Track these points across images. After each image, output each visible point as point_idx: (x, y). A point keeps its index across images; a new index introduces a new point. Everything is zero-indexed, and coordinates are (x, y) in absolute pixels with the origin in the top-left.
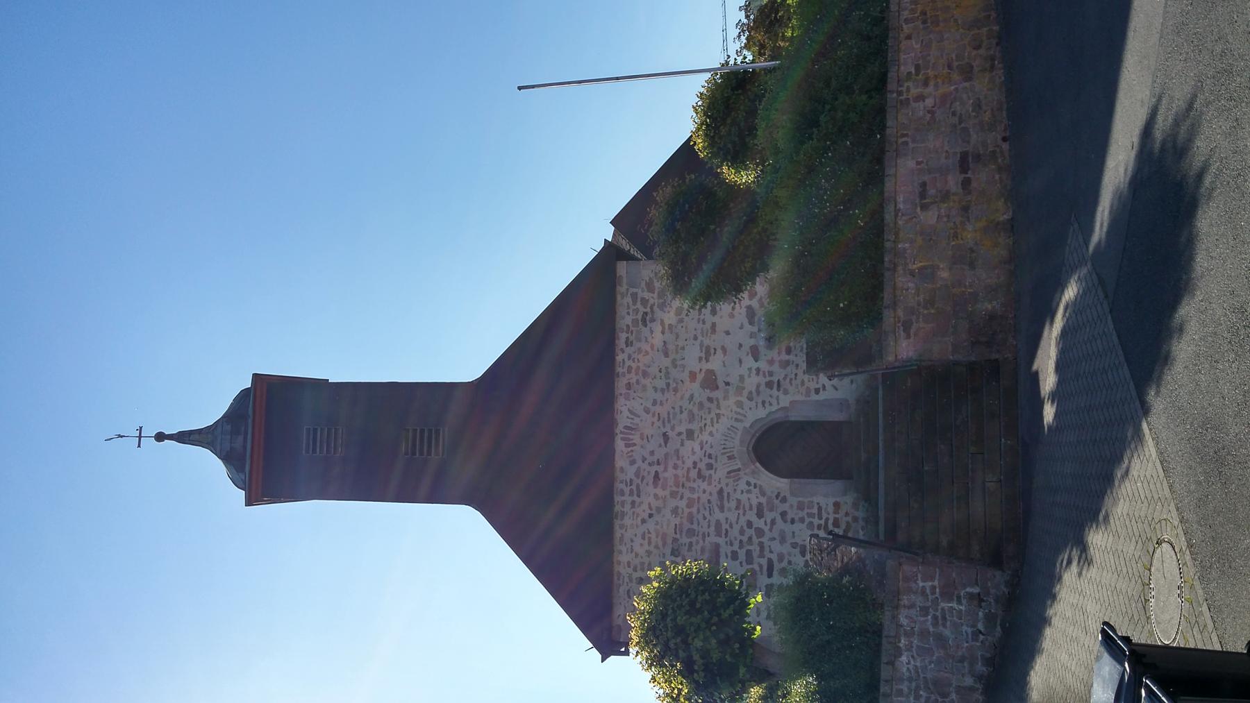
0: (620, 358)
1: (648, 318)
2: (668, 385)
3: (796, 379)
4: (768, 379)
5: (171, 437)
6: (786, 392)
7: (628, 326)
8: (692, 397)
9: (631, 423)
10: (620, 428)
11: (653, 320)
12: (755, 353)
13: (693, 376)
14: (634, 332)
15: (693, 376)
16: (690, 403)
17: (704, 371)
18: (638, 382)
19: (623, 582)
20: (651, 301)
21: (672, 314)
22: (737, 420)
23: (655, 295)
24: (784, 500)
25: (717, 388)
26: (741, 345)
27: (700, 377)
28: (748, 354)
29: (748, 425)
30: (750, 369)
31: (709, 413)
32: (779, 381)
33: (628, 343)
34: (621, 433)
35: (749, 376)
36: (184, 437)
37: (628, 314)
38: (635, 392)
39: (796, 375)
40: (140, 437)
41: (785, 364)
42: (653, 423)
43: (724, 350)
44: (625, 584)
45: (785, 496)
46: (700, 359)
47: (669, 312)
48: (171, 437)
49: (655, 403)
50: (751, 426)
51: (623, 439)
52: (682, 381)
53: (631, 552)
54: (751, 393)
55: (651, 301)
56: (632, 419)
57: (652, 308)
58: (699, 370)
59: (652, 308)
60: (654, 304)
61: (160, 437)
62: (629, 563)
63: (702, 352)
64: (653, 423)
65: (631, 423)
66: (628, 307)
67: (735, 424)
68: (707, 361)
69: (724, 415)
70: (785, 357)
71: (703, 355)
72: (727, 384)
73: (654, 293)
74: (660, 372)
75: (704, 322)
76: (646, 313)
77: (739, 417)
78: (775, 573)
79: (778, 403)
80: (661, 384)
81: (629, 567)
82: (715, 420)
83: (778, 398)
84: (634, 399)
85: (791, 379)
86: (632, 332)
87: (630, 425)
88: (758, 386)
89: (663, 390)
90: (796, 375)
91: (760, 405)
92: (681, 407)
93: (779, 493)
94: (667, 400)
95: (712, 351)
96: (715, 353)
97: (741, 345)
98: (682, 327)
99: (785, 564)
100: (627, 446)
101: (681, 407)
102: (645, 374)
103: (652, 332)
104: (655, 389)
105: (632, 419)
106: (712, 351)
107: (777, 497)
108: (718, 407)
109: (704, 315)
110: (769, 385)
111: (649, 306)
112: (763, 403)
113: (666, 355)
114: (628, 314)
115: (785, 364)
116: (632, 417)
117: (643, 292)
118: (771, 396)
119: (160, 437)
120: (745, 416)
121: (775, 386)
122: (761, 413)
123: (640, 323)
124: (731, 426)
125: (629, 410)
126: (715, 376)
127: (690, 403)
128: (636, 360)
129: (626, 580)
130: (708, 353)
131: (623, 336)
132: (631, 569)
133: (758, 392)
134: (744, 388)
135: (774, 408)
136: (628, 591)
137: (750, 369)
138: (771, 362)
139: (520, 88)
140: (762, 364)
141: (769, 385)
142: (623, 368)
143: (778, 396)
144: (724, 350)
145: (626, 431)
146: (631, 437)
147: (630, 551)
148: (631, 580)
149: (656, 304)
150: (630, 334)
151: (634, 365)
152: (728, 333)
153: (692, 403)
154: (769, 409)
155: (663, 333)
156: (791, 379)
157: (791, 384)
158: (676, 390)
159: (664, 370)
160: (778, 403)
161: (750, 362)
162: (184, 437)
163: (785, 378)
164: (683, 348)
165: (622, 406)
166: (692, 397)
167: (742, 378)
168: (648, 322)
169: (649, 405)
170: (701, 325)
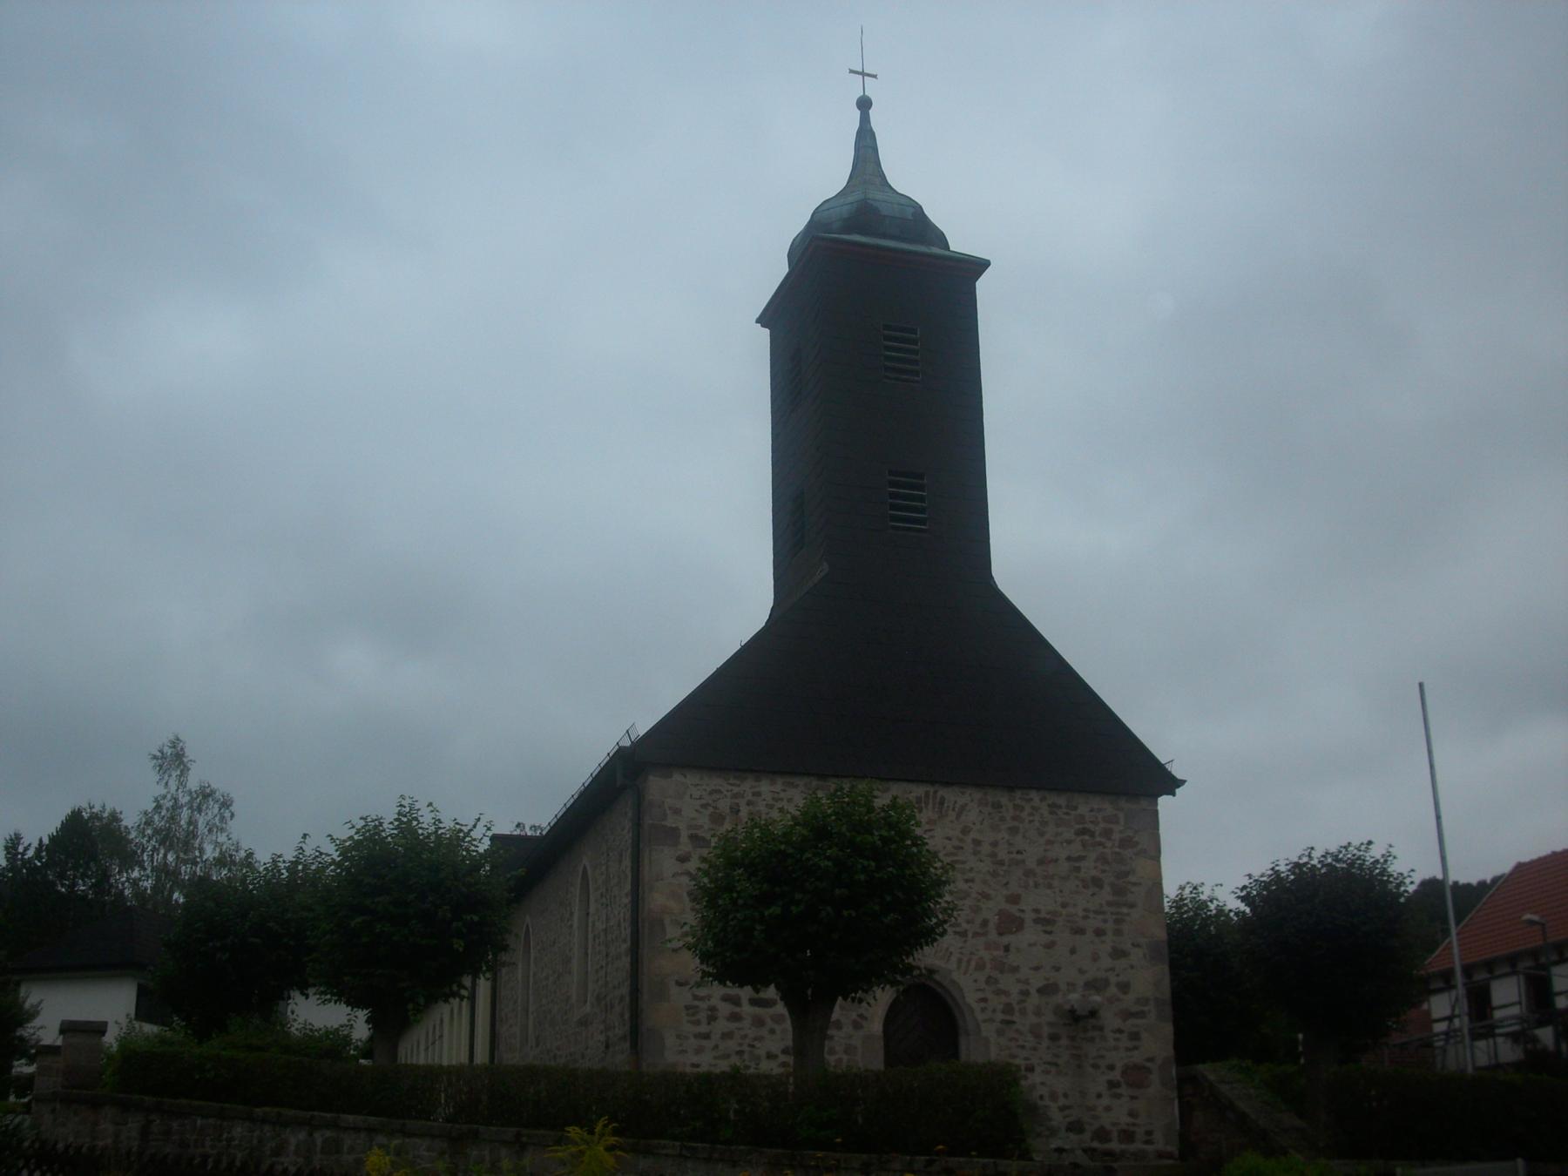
0: (1034, 794)
1: (1087, 837)
2: (1001, 863)
3: (1018, 1046)
4: (1017, 1008)
6: (1000, 1033)
7: (1076, 808)
8: (986, 896)
9: (948, 807)
10: (943, 792)
11: (1084, 845)
12: (1048, 990)
13: (1014, 899)
15: (1014, 899)
16: (980, 894)
17: (1022, 915)
18: (1002, 819)
19: (731, 785)
20: (1109, 844)
21: (1094, 873)
22: (960, 961)
23: (1117, 850)
24: (857, 1026)
25: (1001, 934)
27: (1013, 909)
28: (1047, 979)
29: (955, 976)
30: (1027, 982)
31: (968, 922)
32: (1014, 1022)
33: (1053, 807)
34: (935, 792)
35: (1019, 981)
36: (866, 141)
37: (1092, 811)
38: (990, 814)
39: (1023, 1047)
40: (863, 74)
41: (1035, 1032)
42: (949, 839)
43: (1050, 946)
44: (730, 788)
45: (862, 1027)
46: (1037, 911)
47: (1095, 868)
49: (977, 843)
50: (953, 982)
52: (1007, 883)
53: (773, 799)
55: (1109, 844)
56: (953, 810)
57: (1100, 844)
58: (1024, 908)
59: (1100, 844)
60: (1105, 847)
61: (864, 104)
62: (758, 794)
63: (1048, 913)
64: (949, 839)
65: (948, 807)
66: (1100, 810)
67: (954, 959)
68: (1036, 921)
69: (965, 941)
70: (1046, 1031)
71: (1043, 915)
72: (1007, 949)
73: (1119, 847)
74: (1018, 852)
75: (1085, 918)
76: (1092, 834)
77: (964, 964)
79: (985, 1021)
80: (1002, 854)
81: (754, 794)
82: (958, 929)
83: (991, 1020)
84: (980, 811)
85: (1016, 1040)
86: (1067, 814)
87: (946, 805)
88: (1006, 993)
89: (993, 855)
90: (1023, 1047)
91: (980, 995)
92: (972, 881)
93: (866, 1019)
94: (981, 861)
95: (1049, 928)
96: (1046, 932)
97: (1057, 969)
98: (1077, 886)
99: (770, 1024)
100: (919, 800)
101: (972, 881)
102: (1013, 831)
103: (1069, 842)
104: (995, 844)
105: (953, 810)
106: (1049, 928)
107: (861, 1016)
108: (976, 934)
109: (1094, 918)
110: (1008, 1009)
111: (1103, 840)
112: (984, 1000)
113: (1041, 862)
114: (1092, 811)
115: (1035, 1032)
116: (957, 809)
117: (1121, 832)
118: (994, 1011)
119: (864, 104)
120: (965, 973)
121: (1008, 1018)
122: (971, 998)
123: (1081, 826)
124: (951, 953)
125: (966, 805)
126: (1015, 932)
127: (980, 894)
128: (1031, 818)
129: (736, 790)
130: (1045, 922)
131: (1061, 800)
132: (750, 797)
133: (999, 992)
134: (1002, 972)
135: (980, 1017)
136: (719, 792)
137: (1027, 982)
138: (1038, 1012)
139: (1421, 685)
140: (1034, 1000)
142: (1020, 798)
143: (994, 1021)
144: (1050, 946)
146: (930, 806)
147: (776, 795)
148: (735, 796)
150: (1065, 810)
151: (1024, 815)
152: (1073, 951)
153: (980, 897)
154: (977, 1007)
155: (1069, 859)
156: (1016, 1040)
157: (1011, 1040)
158: (994, 874)
159: (1019, 857)
160: (985, 1021)
161: (1037, 982)
162: (866, 141)
163: (1017, 1031)
164: (1050, 886)
165: (970, 795)
166: (986, 896)
167: (1015, 969)
168: (1082, 837)
169: (973, 835)
170: (1081, 913)
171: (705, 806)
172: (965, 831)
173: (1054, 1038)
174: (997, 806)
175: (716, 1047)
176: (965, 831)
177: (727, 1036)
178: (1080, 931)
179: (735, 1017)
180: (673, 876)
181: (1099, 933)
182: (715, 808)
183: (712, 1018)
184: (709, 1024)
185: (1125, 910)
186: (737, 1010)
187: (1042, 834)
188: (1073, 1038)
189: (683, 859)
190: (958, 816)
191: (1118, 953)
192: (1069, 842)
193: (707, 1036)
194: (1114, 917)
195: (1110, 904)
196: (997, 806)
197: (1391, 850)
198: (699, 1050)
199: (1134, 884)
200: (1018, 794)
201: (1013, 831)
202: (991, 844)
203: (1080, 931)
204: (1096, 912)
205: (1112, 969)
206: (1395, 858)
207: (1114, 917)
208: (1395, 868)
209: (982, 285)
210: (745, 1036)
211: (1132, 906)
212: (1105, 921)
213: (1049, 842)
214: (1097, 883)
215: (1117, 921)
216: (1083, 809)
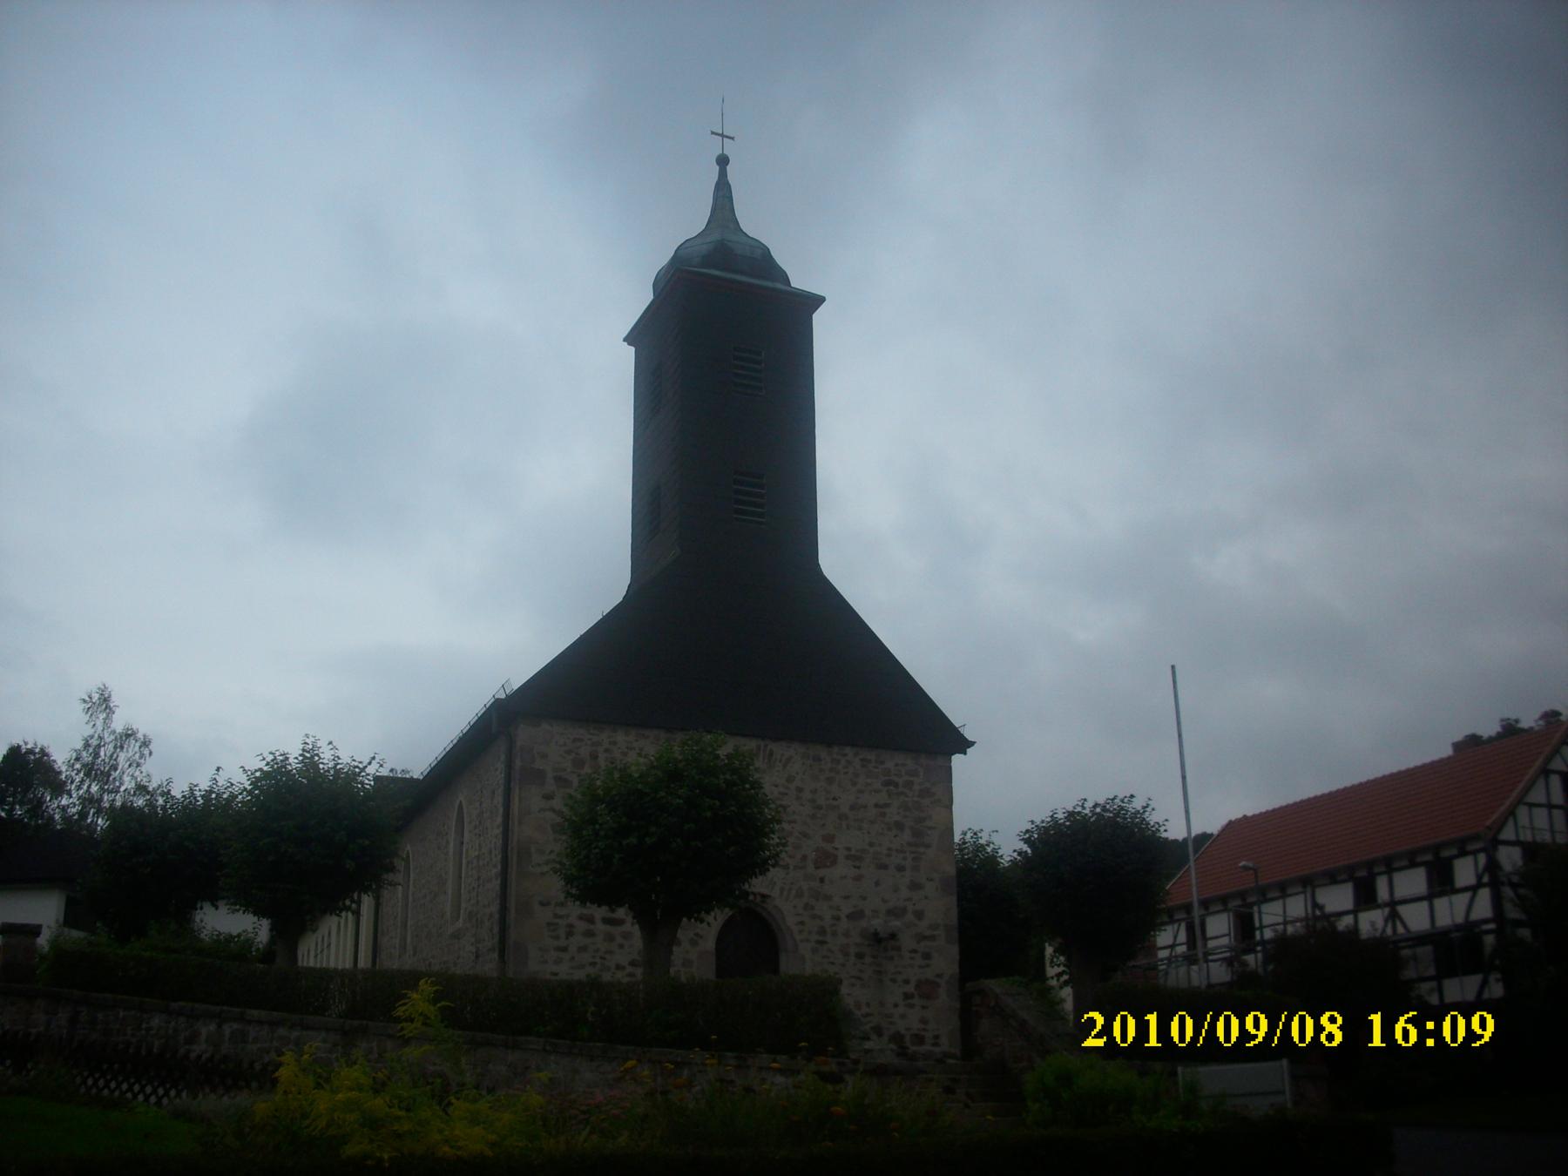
0: (848, 750)
1: (892, 788)
2: (820, 807)
5: (723, 174)
7: (882, 763)
8: (805, 835)
10: (773, 746)
12: (856, 916)
13: (829, 838)
14: (877, 770)
15: (829, 838)
16: (800, 833)
21: (897, 818)
22: (782, 890)
23: (916, 799)
24: (694, 943)
25: (817, 868)
26: (864, 898)
34: (766, 746)
36: (723, 191)
39: (833, 963)
40: (722, 136)
43: (858, 878)
46: (849, 849)
47: (899, 813)
48: (723, 174)
49: (800, 790)
51: (759, 748)
52: (824, 825)
53: (627, 748)
54: (813, 908)
60: (907, 796)
61: (723, 161)
62: (615, 743)
64: (776, 786)
68: (847, 857)
69: (787, 874)
71: (853, 852)
72: (822, 880)
74: (834, 799)
76: (896, 785)
77: (785, 893)
78: (609, 928)
81: (610, 743)
83: (808, 941)
88: (821, 918)
89: (813, 801)
90: (833, 963)
92: (794, 822)
94: (802, 805)
95: (857, 864)
96: (855, 867)
101: (794, 822)
102: (830, 781)
103: (877, 791)
104: (814, 791)
106: (857, 864)
107: (697, 935)
110: (822, 931)
112: (802, 923)
113: (852, 808)
119: (723, 161)
121: (821, 938)
123: (887, 778)
127: (800, 833)
128: (846, 770)
130: (855, 858)
131: (871, 756)
133: (814, 917)
134: (817, 900)
136: (581, 740)
137: (838, 909)
138: (847, 934)
139: (1173, 667)
141: (822, 931)
144: (858, 878)
145: (767, 752)
149: (906, 799)
152: (877, 884)
155: (876, 806)
157: (824, 957)
158: (813, 817)
159: (835, 803)
160: (802, 941)
162: (723, 191)
164: (860, 829)
166: (805, 835)
167: (828, 898)
171: (569, 752)
172: (790, 779)
173: (860, 956)
174: (818, 759)
175: (573, 958)
176: (790, 779)
177: (583, 949)
178: (884, 867)
179: (590, 934)
180: (539, 812)
181: (901, 869)
182: (577, 754)
183: (569, 934)
184: (567, 938)
185: (922, 850)
186: (592, 927)
187: (854, 784)
188: (874, 957)
189: (548, 797)
190: (785, 766)
191: (915, 886)
192: (877, 791)
193: (564, 949)
194: (913, 855)
195: (910, 844)
196: (818, 759)
197: (1150, 802)
198: (558, 962)
199: (930, 828)
200: (836, 749)
201: (830, 781)
202: (811, 791)
203: (884, 867)
204: (897, 850)
205: (910, 899)
206: (1153, 809)
207: (913, 855)
208: (1153, 818)
209: (819, 318)
210: (597, 951)
211: (928, 846)
212: (905, 859)
213: (861, 792)
214: (899, 826)
215: (914, 859)
216: (890, 764)
